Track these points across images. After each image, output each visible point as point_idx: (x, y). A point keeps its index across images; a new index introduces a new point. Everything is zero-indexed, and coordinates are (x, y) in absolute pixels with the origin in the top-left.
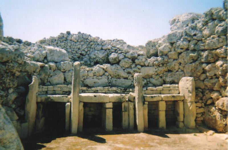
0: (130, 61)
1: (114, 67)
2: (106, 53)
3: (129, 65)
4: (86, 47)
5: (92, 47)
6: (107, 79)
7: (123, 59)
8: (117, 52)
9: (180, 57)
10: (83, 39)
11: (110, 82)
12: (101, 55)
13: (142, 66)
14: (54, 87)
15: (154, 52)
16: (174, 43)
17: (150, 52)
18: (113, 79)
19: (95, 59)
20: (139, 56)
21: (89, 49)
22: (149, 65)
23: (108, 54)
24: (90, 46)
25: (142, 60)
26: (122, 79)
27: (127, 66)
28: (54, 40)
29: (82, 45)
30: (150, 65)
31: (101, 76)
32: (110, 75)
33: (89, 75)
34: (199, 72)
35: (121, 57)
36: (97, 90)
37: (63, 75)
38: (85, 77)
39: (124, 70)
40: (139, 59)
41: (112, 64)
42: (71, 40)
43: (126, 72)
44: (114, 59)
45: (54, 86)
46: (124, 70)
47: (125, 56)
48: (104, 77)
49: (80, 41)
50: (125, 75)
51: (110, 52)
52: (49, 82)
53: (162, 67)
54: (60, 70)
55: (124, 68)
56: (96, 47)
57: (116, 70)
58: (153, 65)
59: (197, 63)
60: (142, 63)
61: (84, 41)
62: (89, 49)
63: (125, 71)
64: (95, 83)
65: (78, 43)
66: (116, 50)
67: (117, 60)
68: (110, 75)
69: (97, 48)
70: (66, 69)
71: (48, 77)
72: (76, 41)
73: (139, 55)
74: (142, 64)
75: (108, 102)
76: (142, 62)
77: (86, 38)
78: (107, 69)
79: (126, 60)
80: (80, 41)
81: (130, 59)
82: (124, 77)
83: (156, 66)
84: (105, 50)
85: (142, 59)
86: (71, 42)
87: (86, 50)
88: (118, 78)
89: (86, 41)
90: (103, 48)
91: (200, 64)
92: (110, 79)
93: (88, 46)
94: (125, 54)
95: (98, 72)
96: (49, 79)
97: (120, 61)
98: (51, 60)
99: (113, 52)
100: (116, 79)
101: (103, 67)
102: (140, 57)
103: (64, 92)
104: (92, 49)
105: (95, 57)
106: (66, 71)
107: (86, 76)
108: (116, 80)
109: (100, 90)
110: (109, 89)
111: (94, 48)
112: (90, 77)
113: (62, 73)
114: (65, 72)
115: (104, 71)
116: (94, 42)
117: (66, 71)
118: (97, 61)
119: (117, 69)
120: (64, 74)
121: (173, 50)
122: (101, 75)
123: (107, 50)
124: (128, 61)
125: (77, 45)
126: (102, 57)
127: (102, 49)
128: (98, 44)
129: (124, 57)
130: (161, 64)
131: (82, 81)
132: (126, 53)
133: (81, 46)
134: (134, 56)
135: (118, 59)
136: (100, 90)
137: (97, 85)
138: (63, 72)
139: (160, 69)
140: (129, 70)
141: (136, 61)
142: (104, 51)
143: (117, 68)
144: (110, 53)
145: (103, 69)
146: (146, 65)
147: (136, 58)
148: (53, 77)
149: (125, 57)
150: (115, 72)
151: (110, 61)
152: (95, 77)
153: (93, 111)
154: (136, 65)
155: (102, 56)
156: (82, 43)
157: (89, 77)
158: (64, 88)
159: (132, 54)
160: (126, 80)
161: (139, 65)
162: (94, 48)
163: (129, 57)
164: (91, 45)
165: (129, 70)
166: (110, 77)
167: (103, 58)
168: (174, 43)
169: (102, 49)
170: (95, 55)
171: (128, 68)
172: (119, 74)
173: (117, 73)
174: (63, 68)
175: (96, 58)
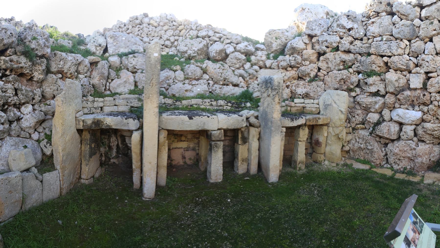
0: (243, 57)
1: (218, 65)
2: (204, 42)
3: (241, 64)
4: (171, 33)
5: (181, 33)
6: (206, 85)
7: (233, 52)
8: (223, 42)
9: (322, 58)
10: (167, 21)
11: (211, 90)
12: (197, 45)
13: (261, 68)
14: (114, 100)
15: (278, 47)
16: (315, 36)
17: (272, 47)
18: (216, 85)
19: (186, 53)
20: (257, 52)
21: (176, 38)
22: (272, 67)
23: (208, 44)
24: (179, 32)
25: (261, 57)
26: (231, 87)
27: (237, 66)
28: (123, 25)
29: (166, 31)
30: (273, 67)
31: (198, 80)
32: (212, 79)
33: (177, 78)
34: (353, 85)
35: (230, 49)
36: (191, 103)
37: (132, 78)
38: (171, 81)
39: (233, 71)
40: (256, 56)
41: (215, 61)
42: (149, 24)
43: (237, 75)
44: (218, 52)
45: (115, 97)
46: (233, 71)
47: (235, 48)
48: (201, 81)
49: (161, 24)
50: (235, 80)
51: (210, 40)
52: (109, 90)
53: (291, 72)
54: (128, 69)
55: (234, 69)
56: (188, 34)
57: (221, 71)
58: (278, 66)
59: (351, 70)
60: (261, 62)
61: (169, 25)
62: (176, 38)
63: (236, 73)
64: (186, 91)
65: (160, 28)
66: (220, 38)
67: (223, 55)
68: (212, 79)
69: (189, 35)
70: (136, 67)
71: (107, 81)
72: (156, 24)
73: (257, 49)
74: (261, 63)
75: (216, 129)
76: (262, 61)
77: (172, 20)
78: (207, 68)
79: (236, 53)
80: (161, 24)
81: (242, 53)
82: (234, 83)
83: (282, 69)
84: (203, 38)
85: (261, 55)
86: (148, 26)
87: (172, 39)
88: (224, 85)
89: (171, 24)
90: (198, 35)
91: (355, 73)
92: (211, 85)
93: (175, 32)
94: (235, 45)
95: (192, 73)
96: (108, 84)
97: (227, 56)
98: (114, 53)
99: (216, 41)
100: (221, 86)
101: (201, 66)
102: (259, 53)
103: (132, 107)
104: (181, 38)
105: (185, 49)
106: (138, 69)
107: (172, 79)
108: (221, 88)
109: (196, 104)
110: (212, 103)
111: (184, 36)
112: (179, 81)
113: (131, 74)
114: (136, 72)
115: (202, 72)
116: (185, 26)
117: (138, 69)
118: (189, 56)
119: (223, 69)
120: (134, 77)
121: (309, 47)
122: (197, 78)
123: (206, 39)
124: (240, 57)
125: (157, 31)
126: (198, 50)
127: (198, 37)
128: (192, 29)
129: (234, 50)
130: (291, 67)
131: (164, 88)
132: (237, 44)
133: (163, 31)
134: (248, 50)
135: (226, 53)
136: (196, 104)
137: (192, 94)
138: (133, 73)
139: (288, 73)
140: (241, 71)
141: (253, 58)
142: (201, 39)
143: (223, 68)
144: (211, 42)
145: (201, 68)
146: (268, 66)
147: (252, 54)
148: (114, 81)
149: (236, 50)
150: (220, 74)
151: (212, 54)
152: (187, 81)
153: (184, 141)
154: (252, 65)
155: (197, 48)
156: (166, 28)
157: (177, 81)
158: (133, 101)
159: (246, 46)
160: (236, 88)
161: (255, 64)
162: (184, 36)
163: (243, 51)
164: (180, 31)
165: (241, 71)
166: (211, 82)
167: (199, 52)
168: (315, 36)
169: (198, 37)
170: (186, 46)
171: (238, 68)
172: (227, 78)
173: (223, 75)
174: (132, 65)
175: (187, 51)
